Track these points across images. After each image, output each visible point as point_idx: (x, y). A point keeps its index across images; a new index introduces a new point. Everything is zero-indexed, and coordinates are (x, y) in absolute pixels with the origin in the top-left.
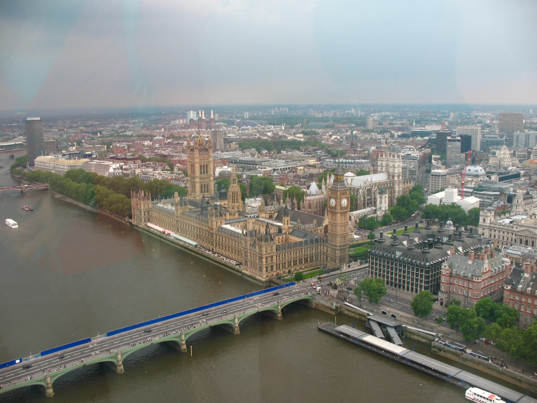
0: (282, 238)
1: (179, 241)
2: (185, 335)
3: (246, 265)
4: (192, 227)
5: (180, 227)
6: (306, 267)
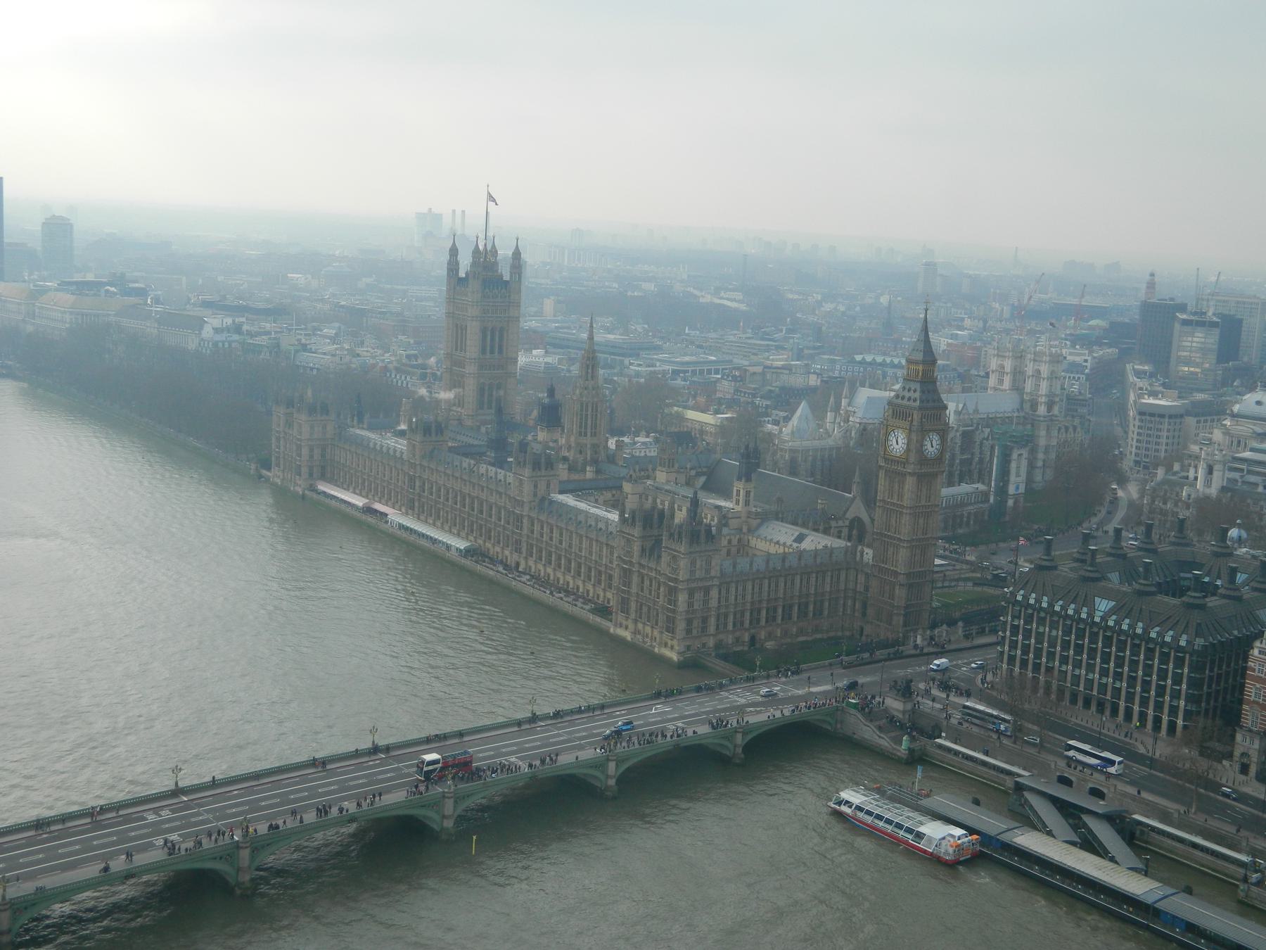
0: (730, 542)
1: (412, 538)
2: (456, 802)
3: (625, 609)
6: (801, 632)
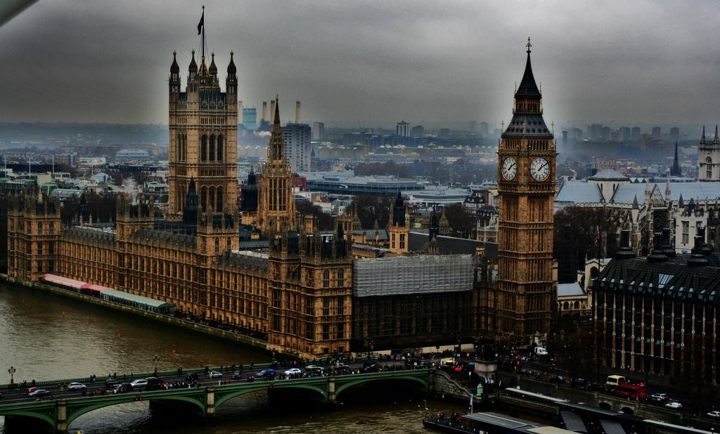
3: (276, 325)
4: (156, 266)
5: (128, 271)
